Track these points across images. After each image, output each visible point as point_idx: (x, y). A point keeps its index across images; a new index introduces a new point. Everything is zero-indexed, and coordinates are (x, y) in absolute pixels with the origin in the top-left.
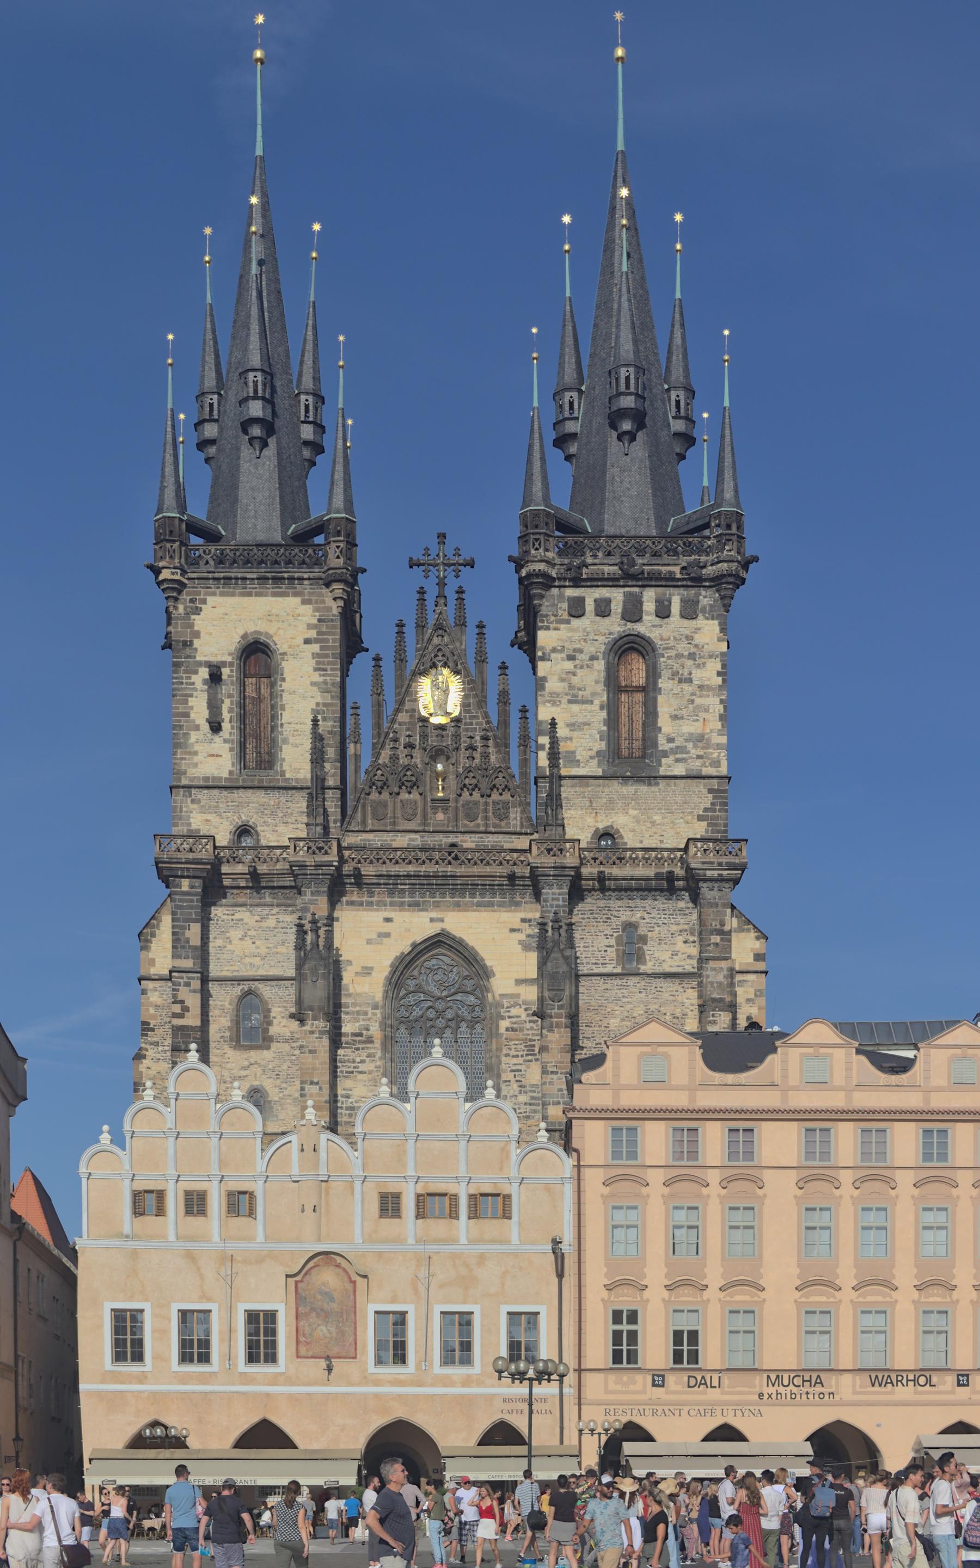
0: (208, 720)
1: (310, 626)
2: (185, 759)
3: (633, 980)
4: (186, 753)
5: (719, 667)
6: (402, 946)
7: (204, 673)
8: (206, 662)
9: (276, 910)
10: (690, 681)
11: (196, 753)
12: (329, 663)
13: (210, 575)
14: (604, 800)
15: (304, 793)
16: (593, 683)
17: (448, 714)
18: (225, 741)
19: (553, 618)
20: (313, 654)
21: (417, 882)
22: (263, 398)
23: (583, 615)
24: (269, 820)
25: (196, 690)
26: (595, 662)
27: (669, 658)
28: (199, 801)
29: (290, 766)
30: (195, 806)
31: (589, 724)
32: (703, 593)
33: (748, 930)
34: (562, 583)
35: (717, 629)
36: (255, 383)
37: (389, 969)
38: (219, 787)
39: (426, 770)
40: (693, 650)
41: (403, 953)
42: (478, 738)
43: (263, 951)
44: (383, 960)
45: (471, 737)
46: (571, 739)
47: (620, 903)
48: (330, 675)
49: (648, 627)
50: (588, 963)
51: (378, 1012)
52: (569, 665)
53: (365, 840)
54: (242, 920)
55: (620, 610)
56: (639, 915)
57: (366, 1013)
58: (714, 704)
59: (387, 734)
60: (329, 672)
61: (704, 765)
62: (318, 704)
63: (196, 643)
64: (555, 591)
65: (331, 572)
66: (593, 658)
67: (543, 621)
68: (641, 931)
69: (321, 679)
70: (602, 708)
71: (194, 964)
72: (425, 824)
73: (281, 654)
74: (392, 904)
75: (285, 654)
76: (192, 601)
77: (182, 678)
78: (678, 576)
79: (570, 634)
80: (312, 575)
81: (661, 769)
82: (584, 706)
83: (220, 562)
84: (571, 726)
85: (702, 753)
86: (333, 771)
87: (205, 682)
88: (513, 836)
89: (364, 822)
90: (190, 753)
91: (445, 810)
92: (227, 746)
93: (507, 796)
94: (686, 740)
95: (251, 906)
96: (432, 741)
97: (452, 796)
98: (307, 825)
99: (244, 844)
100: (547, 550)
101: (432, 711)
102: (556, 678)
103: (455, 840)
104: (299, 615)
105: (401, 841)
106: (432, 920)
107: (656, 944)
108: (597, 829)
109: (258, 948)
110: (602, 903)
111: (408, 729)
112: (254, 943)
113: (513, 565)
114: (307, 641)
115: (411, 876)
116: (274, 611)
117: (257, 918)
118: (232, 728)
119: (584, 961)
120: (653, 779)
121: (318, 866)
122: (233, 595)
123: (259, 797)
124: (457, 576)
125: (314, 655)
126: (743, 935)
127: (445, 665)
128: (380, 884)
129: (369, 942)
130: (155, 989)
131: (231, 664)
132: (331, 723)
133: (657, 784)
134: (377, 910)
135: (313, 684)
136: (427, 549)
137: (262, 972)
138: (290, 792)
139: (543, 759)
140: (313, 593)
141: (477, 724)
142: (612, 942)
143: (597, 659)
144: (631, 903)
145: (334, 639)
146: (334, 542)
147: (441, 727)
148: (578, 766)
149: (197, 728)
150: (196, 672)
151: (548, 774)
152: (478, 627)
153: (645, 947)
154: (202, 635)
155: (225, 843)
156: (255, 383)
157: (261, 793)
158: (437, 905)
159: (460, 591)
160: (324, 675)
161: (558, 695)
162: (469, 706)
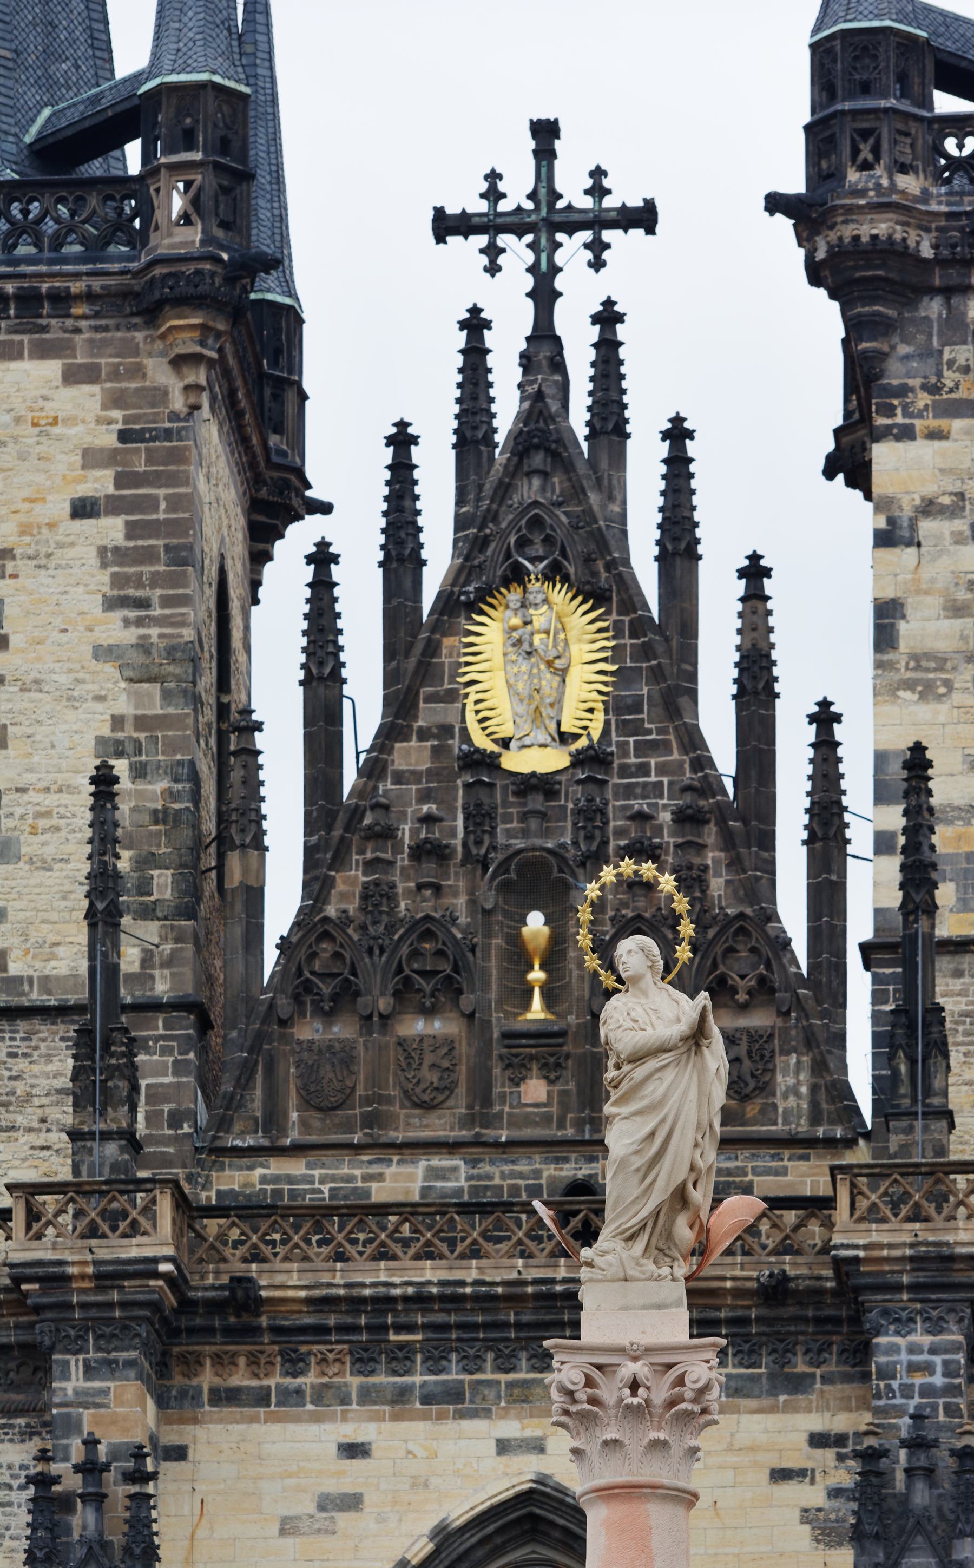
1: (92, 458)
17: (564, 738)
19: (923, 399)
20: (102, 551)
21: (453, 1319)
29: (25, 936)
34: (954, 275)
39: (488, 935)
42: (666, 817)
45: (641, 817)
53: (276, 1179)
60: (157, 612)
62: (117, 722)
64: (934, 308)
65: (158, 271)
67: (889, 411)
69: (131, 635)
72: (489, 1121)
74: (367, 1396)
80: (97, 284)
86: (168, 947)
88: (786, 1153)
89: (273, 1120)
91: (552, 1070)
96: (509, 835)
98: (75, 1135)
101: (506, 730)
102: (934, 603)
104: (55, 422)
105: (401, 1181)
106: (503, 1447)
111: (425, 796)
113: (784, 225)
114: (83, 509)
115: (430, 1298)
121: (108, 1276)
127: (554, 574)
128: (325, 1330)
129: (288, 1527)
132: (161, 785)
134: (316, 1419)
135: (102, 653)
136: (493, 176)
138: (23, 1026)
140: (104, 343)
160: (139, 622)
161: (941, 662)
162: (636, 707)
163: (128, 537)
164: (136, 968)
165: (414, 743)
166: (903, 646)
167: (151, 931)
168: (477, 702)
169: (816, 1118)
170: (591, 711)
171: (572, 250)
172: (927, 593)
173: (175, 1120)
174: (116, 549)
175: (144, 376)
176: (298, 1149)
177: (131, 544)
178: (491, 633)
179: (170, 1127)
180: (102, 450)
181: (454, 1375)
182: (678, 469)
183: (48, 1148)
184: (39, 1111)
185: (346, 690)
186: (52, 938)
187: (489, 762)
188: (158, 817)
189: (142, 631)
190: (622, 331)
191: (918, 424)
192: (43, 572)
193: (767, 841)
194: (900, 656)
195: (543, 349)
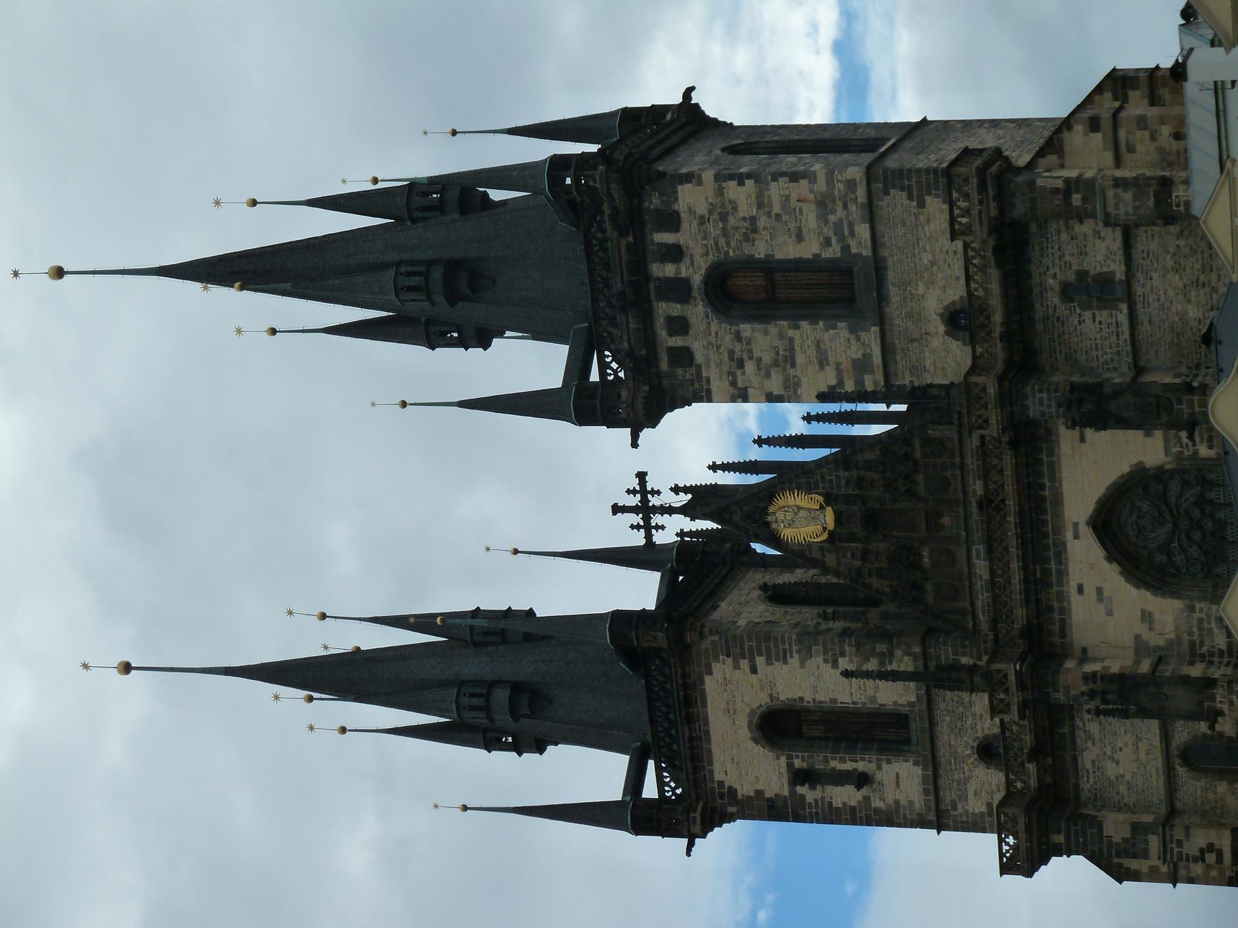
0: (859, 787)
1: (736, 666)
3: (1139, 290)
5: (732, 184)
6: (1111, 576)
9: (1078, 722)
10: (753, 220)
11: (897, 802)
12: (776, 646)
13: (691, 777)
14: (909, 324)
15: (934, 691)
17: (822, 507)
18: (879, 768)
19: (697, 386)
20: (768, 664)
22: (487, 701)
24: (969, 722)
25: (823, 798)
27: (728, 245)
30: (959, 806)
31: (818, 343)
32: (646, 204)
33: (1061, 141)
35: (688, 186)
36: (472, 708)
37: (1143, 591)
40: (716, 216)
41: (1121, 573)
43: (1129, 739)
44: (1131, 600)
45: (848, 483)
46: (838, 364)
47: (1037, 306)
48: (790, 645)
49: (695, 270)
50: (1118, 345)
51: (1198, 606)
52: (750, 367)
54: (1093, 762)
55: (679, 306)
56: (1051, 281)
57: (1200, 620)
58: (776, 190)
61: (855, 200)
63: (768, 795)
64: (665, 382)
66: (738, 337)
68: (1071, 277)
69: (796, 655)
70: (797, 327)
71: (1154, 834)
74: (1060, 584)
75: (771, 696)
77: (811, 813)
78: (631, 239)
79: (713, 366)
81: (864, 253)
84: (822, 363)
85: (840, 204)
87: (813, 787)
92: (884, 766)
93: (917, 443)
94: (826, 222)
95: (1075, 749)
98: (972, 691)
99: (1001, 750)
100: (619, 397)
101: (820, 527)
102: (766, 382)
103: (974, 504)
105: (981, 567)
106: (1076, 537)
107: (1087, 259)
108: (946, 333)
109: (1126, 745)
110: (1040, 327)
111: (845, 556)
112: (1121, 749)
114: (754, 670)
116: (723, 706)
117: (1089, 744)
118: (863, 759)
119: (1116, 349)
120: (878, 265)
122: (710, 751)
123: (943, 731)
124: (658, 493)
126: (1067, 148)
127: (765, 511)
129: (1109, 613)
130: (1188, 868)
131: (789, 757)
132: (847, 648)
133: (884, 259)
134: (1069, 601)
136: (632, 527)
137: (1157, 742)
141: (830, 475)
142: (1087, 315)
144: (1036, 290)
146: (638, 641)
148: (870, 356)
149: (867, 799)
150: (803, 797)
152: (715, 471)
153: (1092, 273)
156: (472, 708)
158: (1058, 531)
159: (676, 490)
160: (791, 653)
161: (786, 380)
167: (898, 653)
169: (950, 423)
173: (964, 646)
176: (972, 604)
178: (787, 533)
181: (1051, 554)
182: (726, 467)
187: (831, 534)
188: (858, 647)
190: (681, 485)
193: (853, 439)
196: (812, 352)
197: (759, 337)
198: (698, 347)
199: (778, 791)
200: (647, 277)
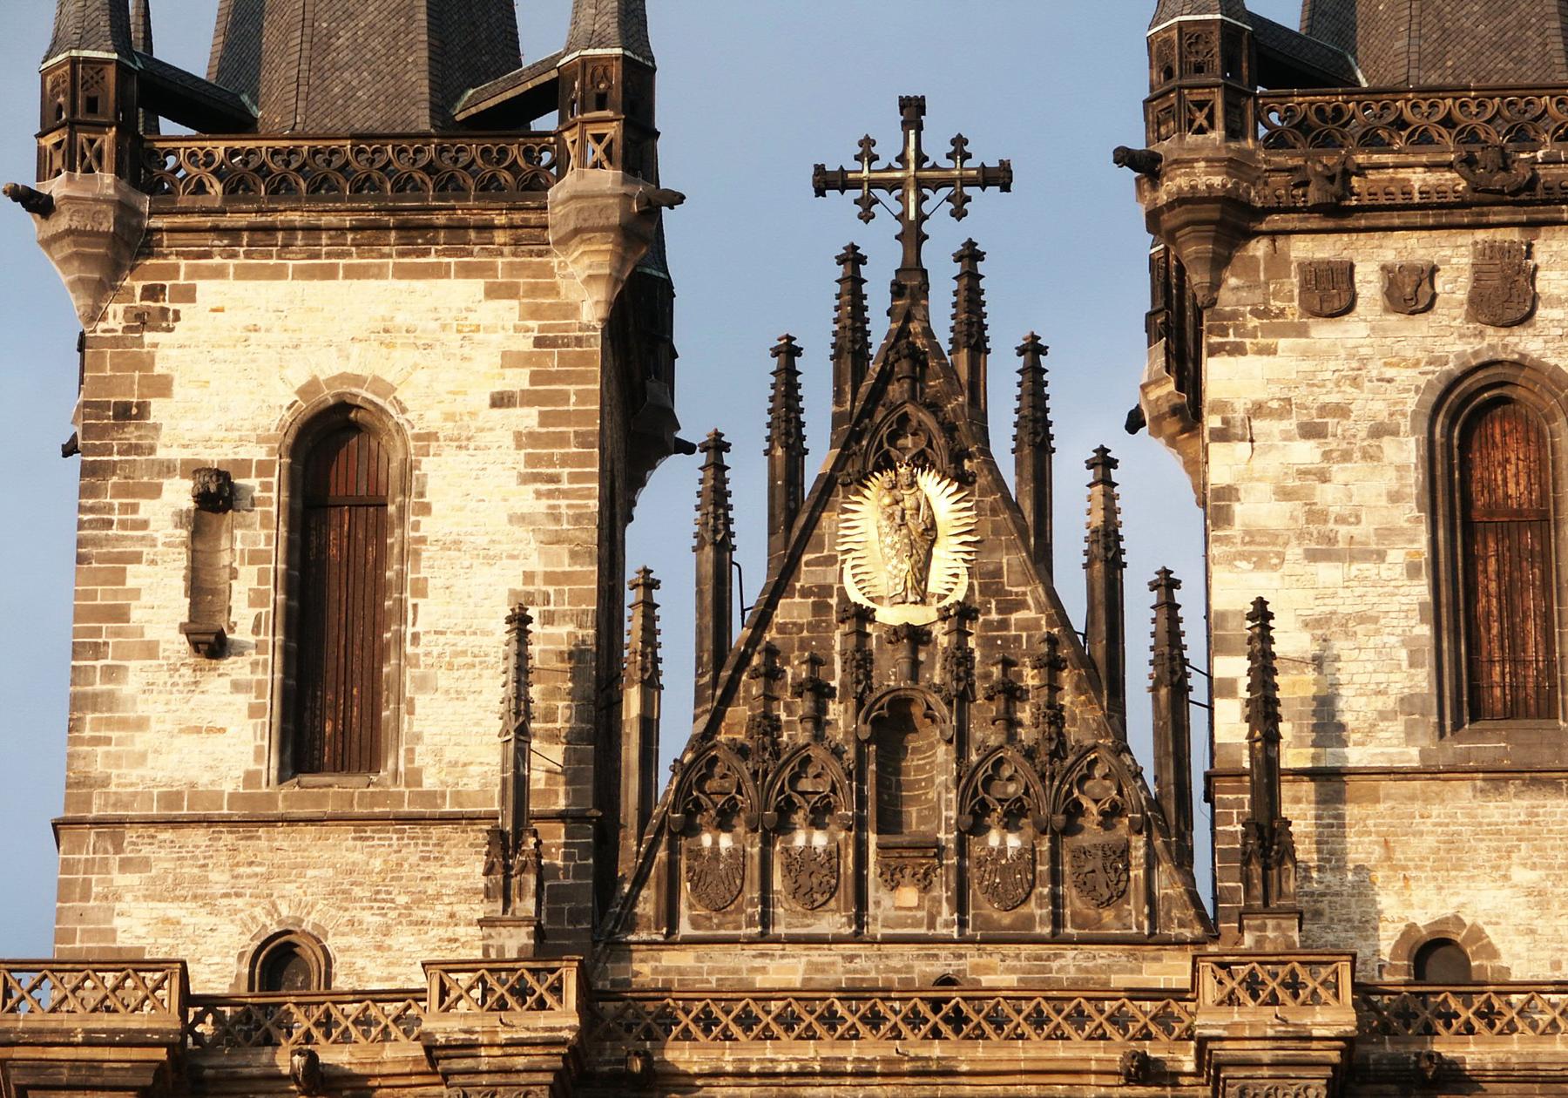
0: (186, 630)
1: (510, 359)
2: (108, 741)
4: (109, 723)
7: (180, 494)
8: (185, 463)
11: (141, 724)
12: (565, 461)
13: (208, 221)
16: (1384, 501)
18: (237, 687)
19: (1253, 322)
20: (518, 436)
23: (1349, 309)
26: (1386, 441)
28: (145, 864)
31: (1375, 620)
38: (209, 822)
48: (565, 494)
52: (1307, 452)
53: (668, 970)
55: (1462, 295)
59: (744, 660)
60: (565, 485)
62: (529, 577)
63: (158, 409)
64: (1259, 248)
66: (1378, 431)
69: (542, 505)
70: (1413, 571)
73: (418, 437)
75: (431, 436)
76: (152, 293)
77: (111, 509)
79: (1307, 366)
82: (1355, 569)
83: (237, 185)
87: (181, 518)
90: (124, 724)
92: (244, 700)
97: (947, 837)
102: (1266, 488)
104: (478, 328)
114: (501, 401)
115: (813, 1074)
116: (401, 319)
122: (278, 274)
123: (343, 850)
124: (959, 214)
125: (521, 439)
131: (264, 468)
138: (436, 832)
139: (1231, 724)
143: (1395, 433)
145: (584, 394)
147: (916, 636)
150: (154, 492)
151: (1247, 765)
154: (176, 388)
155: (220, 987)
157: (346, 835)
159: (970, 255)
160: (550, 494)
161: (1273, 537)
163: (541, 424)
164: (542, 786)
165: (797, 599)
166: (1238, 521)
168: (853, 567)
170: (956, 575)
171: (937, 200)
172: (1258, 480)
173: (575, 917)
174: (531, 434)
175: (558, 293)
177: (544, 430)
179: (570, 922)
180: (519, 352)
183: (456, 940)
184: (449, 909)
185: (736, 557)
186: (463, 759)
189: (552, 502)
191: (1248, 341)
192: (464, 452)
194: (1235, 530)
195: (910, 285)
196: (1346, 604)
197: (1387, 480)
198: (1352, 332)
199: (164, 430)
200: (1534, 225)
